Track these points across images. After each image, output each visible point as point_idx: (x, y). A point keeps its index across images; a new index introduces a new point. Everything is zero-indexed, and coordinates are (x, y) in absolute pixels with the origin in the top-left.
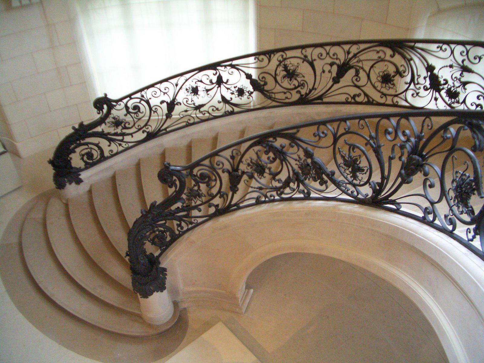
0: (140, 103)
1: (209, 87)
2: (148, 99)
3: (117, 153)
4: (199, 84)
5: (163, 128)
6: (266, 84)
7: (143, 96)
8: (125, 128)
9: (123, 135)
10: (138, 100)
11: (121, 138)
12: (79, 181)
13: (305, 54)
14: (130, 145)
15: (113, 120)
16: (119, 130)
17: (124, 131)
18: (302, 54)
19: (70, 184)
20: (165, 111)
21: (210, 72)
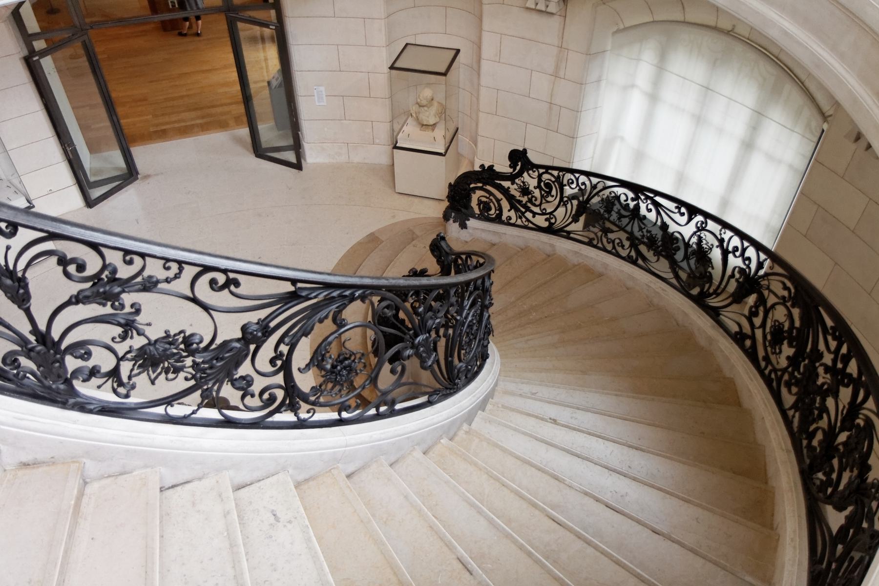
0: (553, 182)
3: (514, 225)
8: (530, 201)
9: (528, 209)
10: (553, 179)
11: (523, 210)
12: (463, 226)
13: (723, 236)
14: (530, 225)
15: (522, 184)
16: (525, 199)
17: (529, 205)
18: (721, 234)
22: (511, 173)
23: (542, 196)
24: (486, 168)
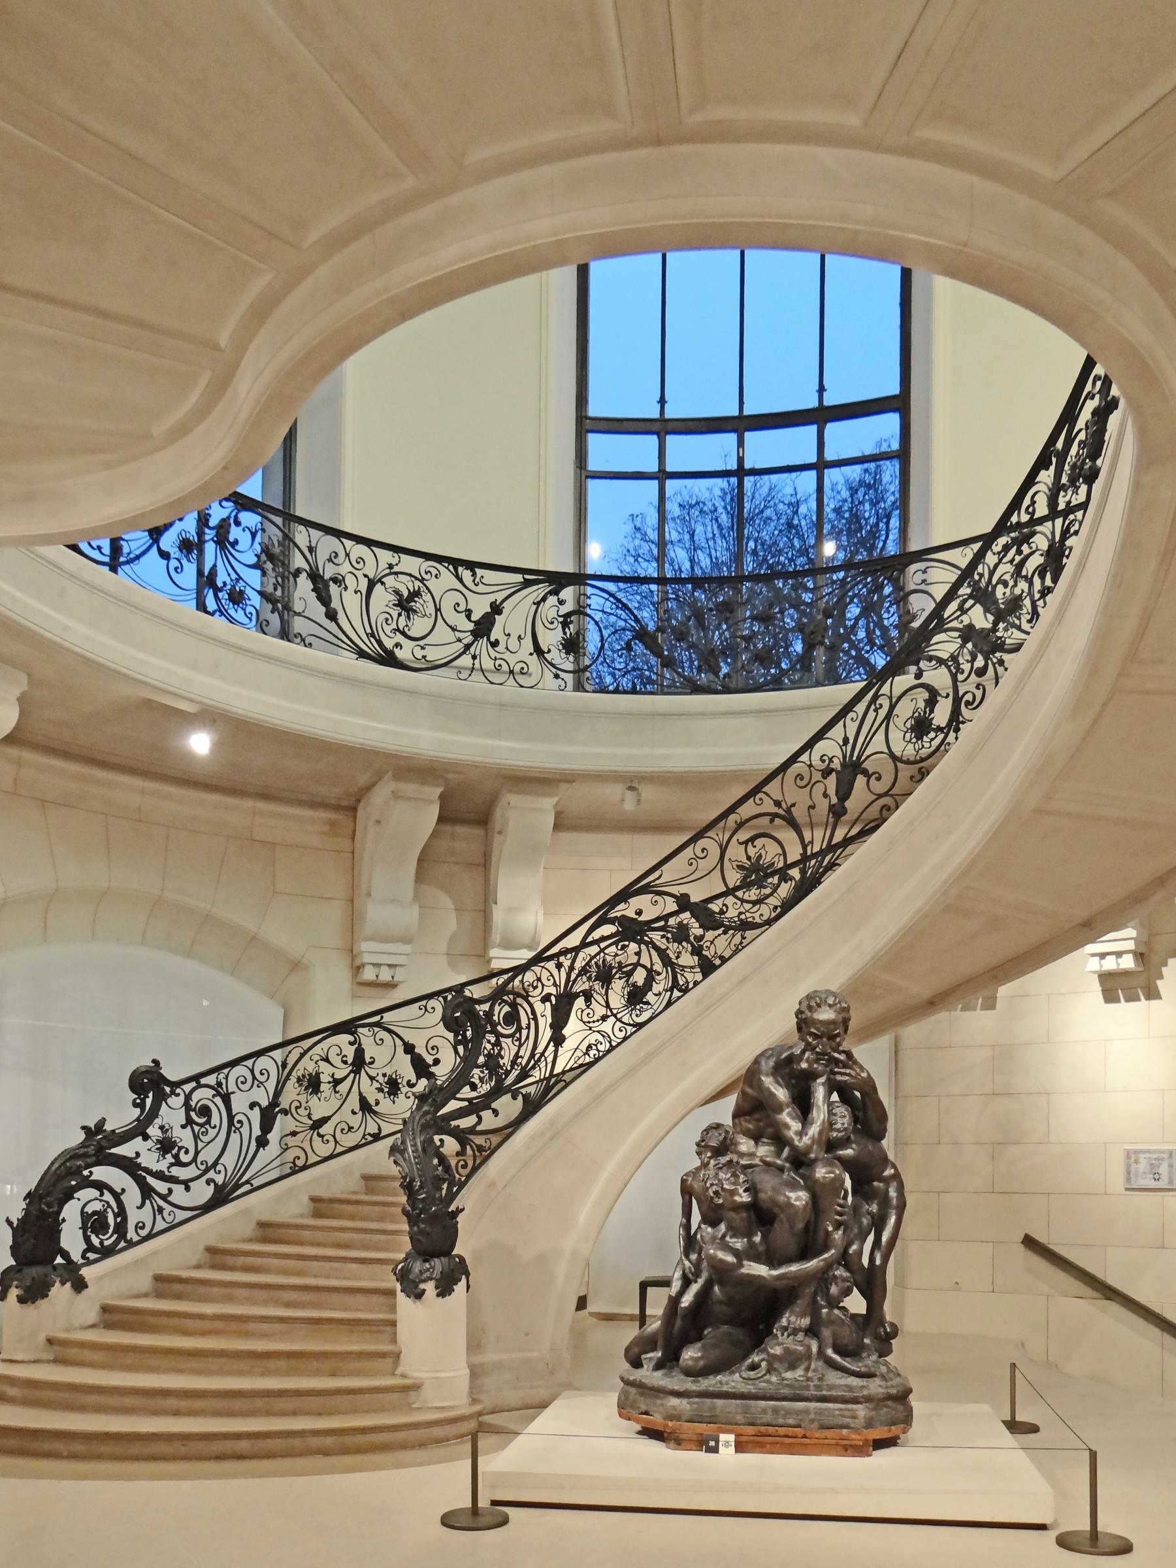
1: (339, 1075)
2: (230, 1091)
4: (324, 1066)
5: (243, 1180)
6: (437, 1062)
7: (219, 1084)
8: (178, 1163)
17: (176, 1171)
19: (63, 1283)
20: (257, 1132)
21: (344, 1038)
22: (138, 1119)
23: (196, 1137)
24: (93, 1129)
